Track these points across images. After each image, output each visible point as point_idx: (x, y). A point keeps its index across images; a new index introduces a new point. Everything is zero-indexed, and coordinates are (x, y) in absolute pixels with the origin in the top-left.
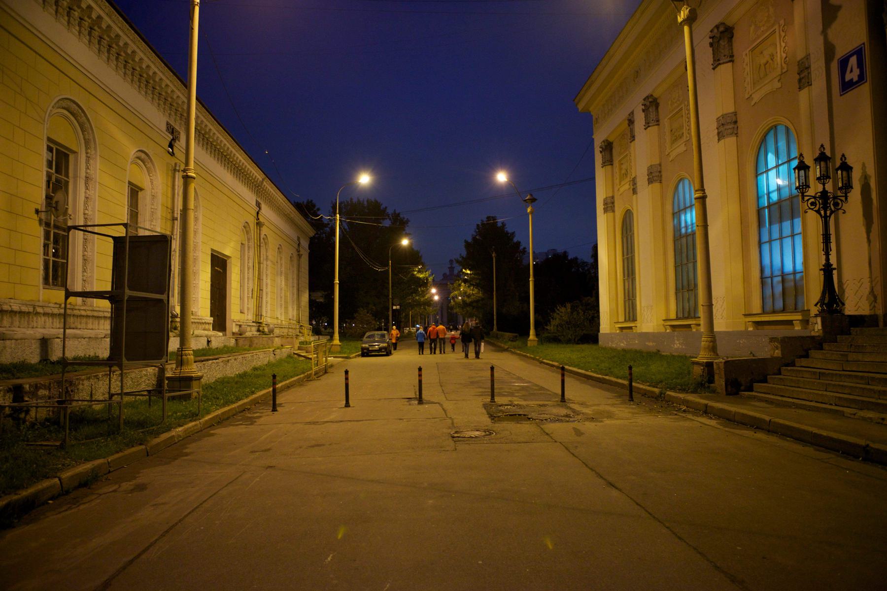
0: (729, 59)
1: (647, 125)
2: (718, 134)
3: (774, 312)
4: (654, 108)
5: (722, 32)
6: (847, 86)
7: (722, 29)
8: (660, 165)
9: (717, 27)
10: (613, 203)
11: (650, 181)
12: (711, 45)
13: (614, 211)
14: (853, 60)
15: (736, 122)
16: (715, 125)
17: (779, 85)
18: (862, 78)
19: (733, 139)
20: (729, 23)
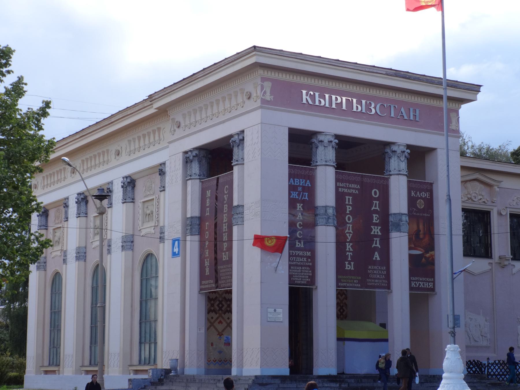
0: (131, 200)
1: (79, 215)
2: (122, 246)
3: (145, 364)
4: (84, 203)
5: (128, 182)
6: (174, 254)
7: (129, 180)
8: (86, 247)
9: (127, 177)
10: (45, 263)
11: (78, 258)
12: (122, 187)
13: (45, 270)
14: (177, 242)
15: (132, 242)
16: (121, 241)
17: (153, 231)
18: (178, 254)
19: (130, 252)
20: (134, 177)
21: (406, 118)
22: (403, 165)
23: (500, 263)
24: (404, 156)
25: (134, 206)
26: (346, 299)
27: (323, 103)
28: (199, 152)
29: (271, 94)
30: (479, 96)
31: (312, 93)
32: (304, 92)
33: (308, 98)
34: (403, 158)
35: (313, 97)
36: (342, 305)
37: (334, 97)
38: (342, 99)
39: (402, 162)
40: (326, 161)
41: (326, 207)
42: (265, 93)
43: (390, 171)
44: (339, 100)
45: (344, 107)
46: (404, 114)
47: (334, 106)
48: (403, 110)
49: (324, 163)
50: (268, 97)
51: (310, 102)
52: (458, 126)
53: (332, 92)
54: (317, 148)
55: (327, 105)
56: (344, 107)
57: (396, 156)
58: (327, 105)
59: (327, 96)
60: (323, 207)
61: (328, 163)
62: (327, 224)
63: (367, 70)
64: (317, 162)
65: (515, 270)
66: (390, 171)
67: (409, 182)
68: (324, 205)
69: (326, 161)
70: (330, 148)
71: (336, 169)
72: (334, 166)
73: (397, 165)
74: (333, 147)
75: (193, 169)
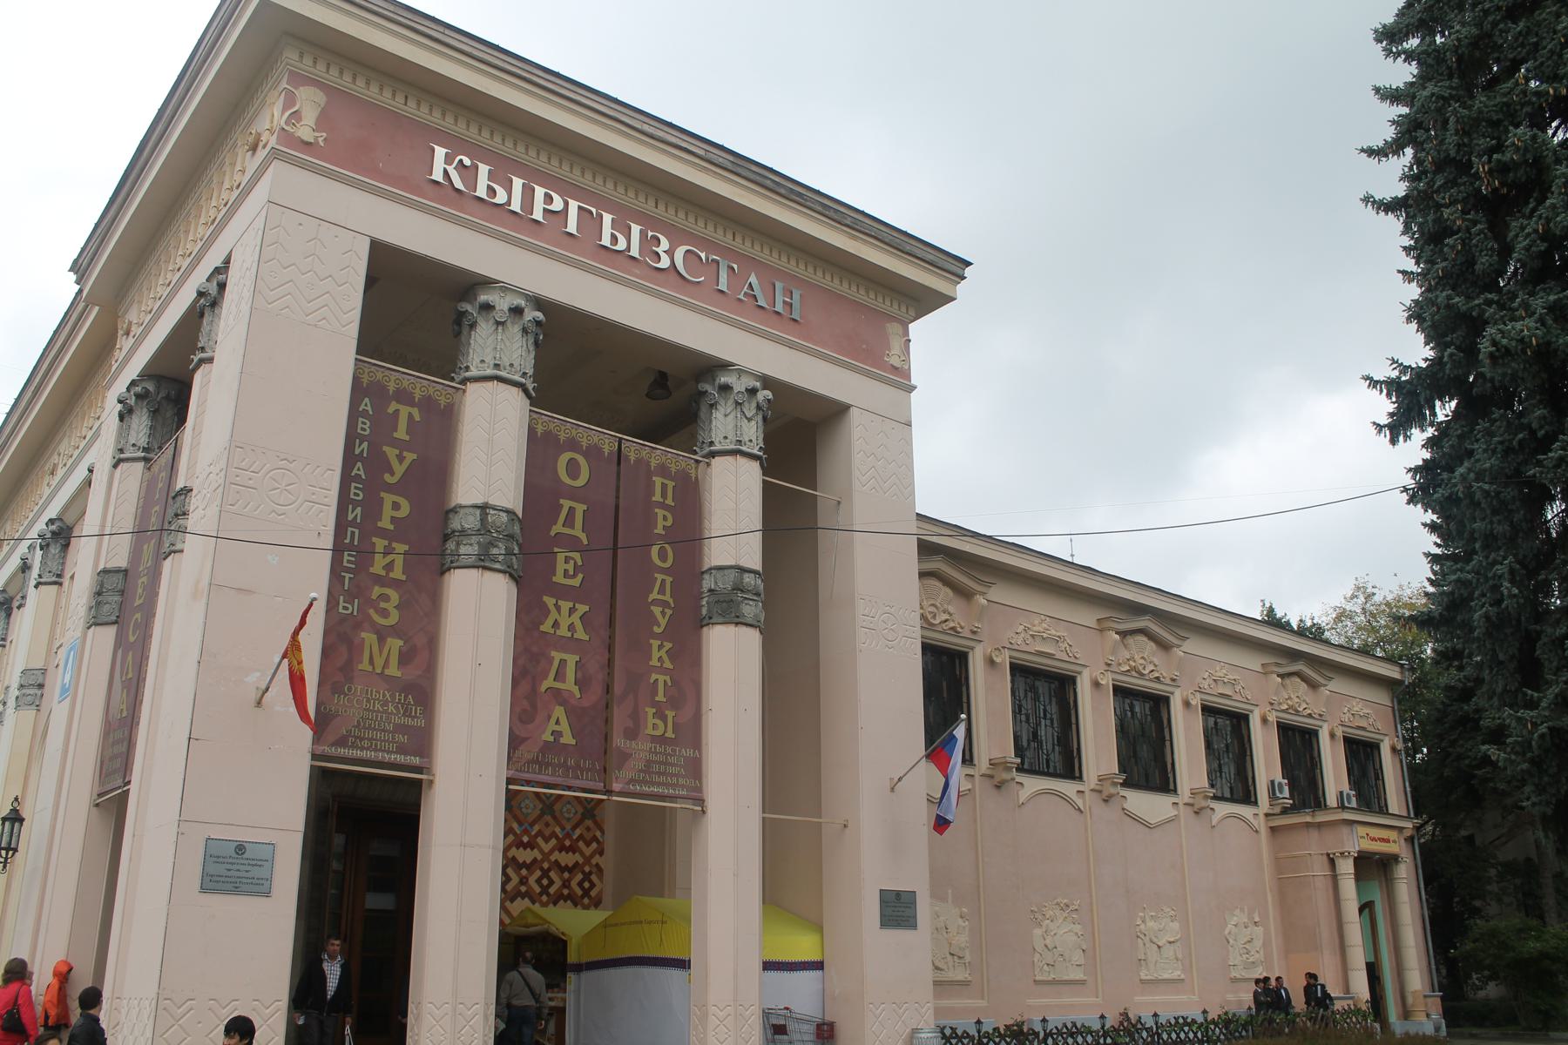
15: (41, 686)
21: (761, 302)
22: (752, 434)
23: (992, 777)
24: (754, 405)
25: (59, 594)
26: (601, 853)
27: (501, 197)
28: (158, 388)
29: (320, 124)
30: (962, 289)
31: (467, 162)
32: (440, 152)
33: (451, 170)
34: (750, 410)
35: (469, 173)
36: (587, 869)
37: (540, 192)
38: (566, 204)
39: (749, 420)
40: (497, 366)
41: (484, 508)
42: (296, 116)
43: (712, 443)
44: (557, 204)
45: (572, 227)
46: (757, 292)
47: (538, 215)
48: (753, 279)
49: (490, 372)
50: (305, 132)
51: (458, 184)
52: (907, 360)
53: (534, 176)
54: (473, 326)
55: (516, 206)
56: (572, 227)
57: (731, 402)
58: (516, 206)
59: (518, 183)
60: (475, 506)
61: (503, 374)
62: (483, 563)
63: (646, 128)
64: (467, 368)
65: (1024, 795)
66: (712, 443)
67: (767, 489)
68: (479, 501)
69: (497, 366)
70: (515, 330)
71: (538, 400)
72: (526, 391)
73: (730, 424)
74: (525, 331)
75: (133, 433)
